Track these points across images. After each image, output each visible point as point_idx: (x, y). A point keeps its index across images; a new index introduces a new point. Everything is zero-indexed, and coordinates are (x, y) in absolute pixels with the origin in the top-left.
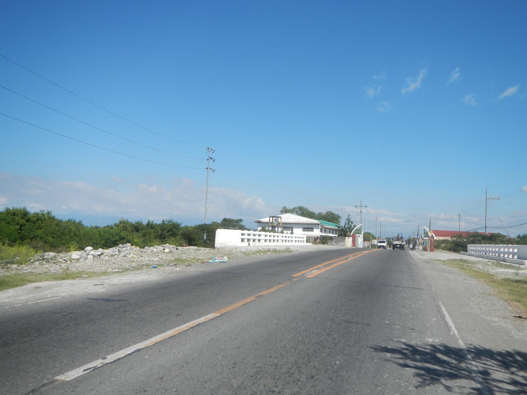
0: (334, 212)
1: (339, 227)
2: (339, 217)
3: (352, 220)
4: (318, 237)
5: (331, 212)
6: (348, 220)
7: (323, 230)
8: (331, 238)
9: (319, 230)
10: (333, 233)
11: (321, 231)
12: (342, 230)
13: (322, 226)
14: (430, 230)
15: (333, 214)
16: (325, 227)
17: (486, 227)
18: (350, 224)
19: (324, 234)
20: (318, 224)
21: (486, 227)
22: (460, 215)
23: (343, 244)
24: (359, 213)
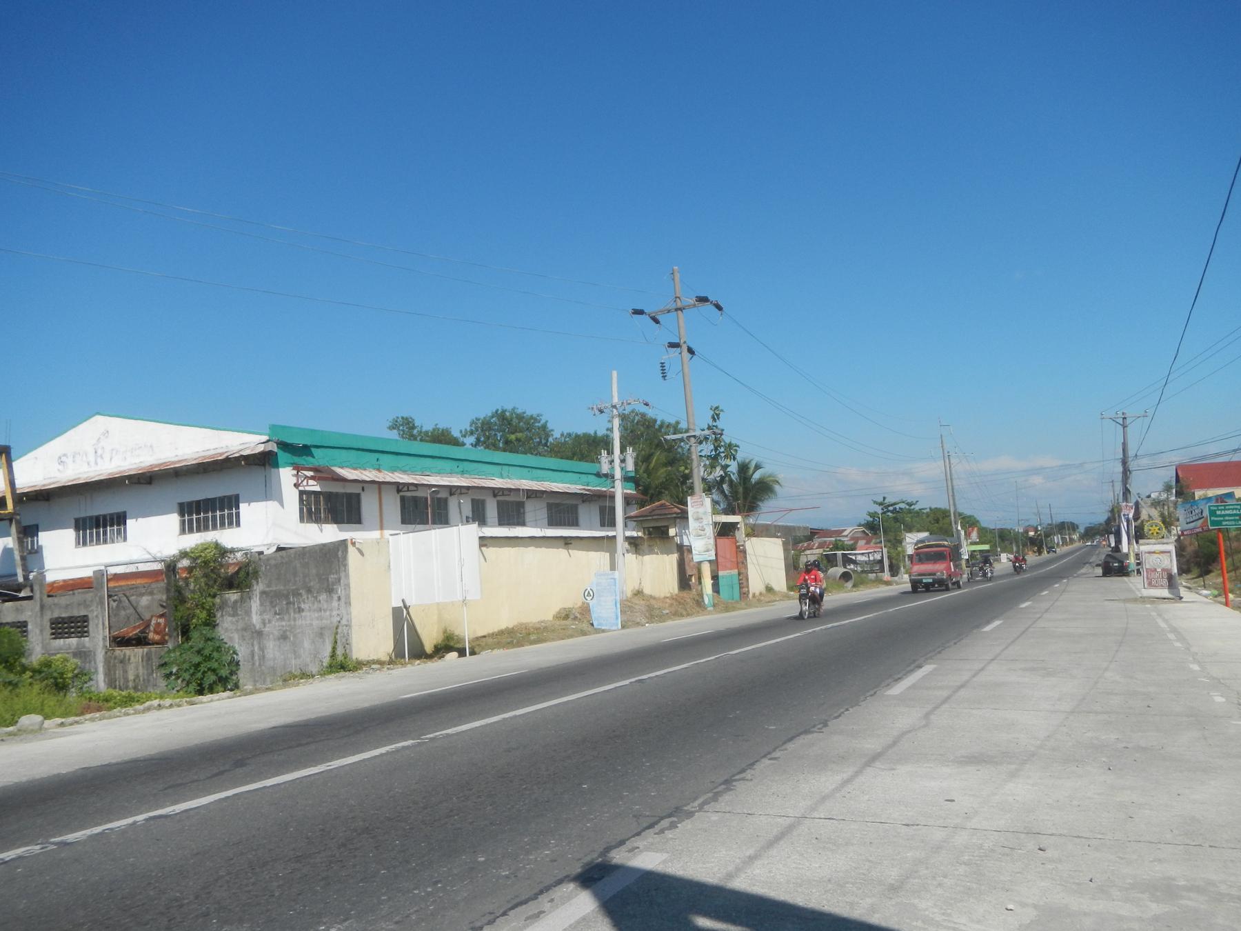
13: (321, 473)
20: (264, 461)
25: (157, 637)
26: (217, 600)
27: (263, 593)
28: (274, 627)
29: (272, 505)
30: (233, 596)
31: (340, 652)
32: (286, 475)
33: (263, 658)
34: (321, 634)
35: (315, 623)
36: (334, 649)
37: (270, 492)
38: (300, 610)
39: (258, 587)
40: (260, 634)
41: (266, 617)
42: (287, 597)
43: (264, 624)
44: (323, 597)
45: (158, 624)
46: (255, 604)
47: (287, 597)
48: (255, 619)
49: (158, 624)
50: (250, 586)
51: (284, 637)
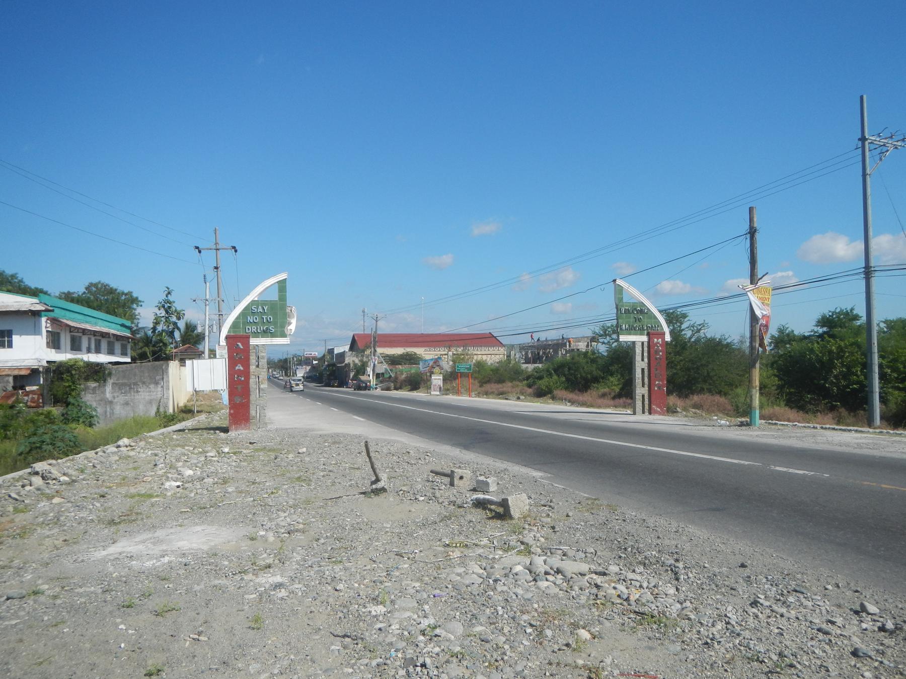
0: (113, 285)
1: (134, 333)
2: (135, 300)
3: (177, 306)
4: (34, 372)
5: (105, 286)
6: (167, 307)
7: (65, 340)
8: (97, 372)
9: (40, 341)
10: (111, 352)
11: (54, 342)
12: (147, 341)
13: (54, 321)
14: (753, 279)
15: (112, 291)
16: (71, 329)
17: (868, 272)
18: (174, 319)
19: (63, 356)
20: (36, 314)
21: (868, 272)
22: (363, 312)
23: (156, 392)
24: (211, 274)
25: (33, 405)
26: (82, 386)
27: (113, 384)
28: (121, 399)
29: (38, 337)
30: (92, 384)
31: (162, 410)
32: (44, 319)
33: (112, 413)
34: (150, 402)
35: (147, 398)
36: (158, 409)
37: (36, 331)
38: (138, 392)
39: (110, 382)
40: (111, 402)
41: (116, 395)
42: (130, 386)
43: (114, 397)
44: (152, 386)
45: (33, 398)
46: (109, 388)
47: (130, 386)
48: (108, 395)
49: (33, 398)
50: (105, 381)
51: (127, 404)
